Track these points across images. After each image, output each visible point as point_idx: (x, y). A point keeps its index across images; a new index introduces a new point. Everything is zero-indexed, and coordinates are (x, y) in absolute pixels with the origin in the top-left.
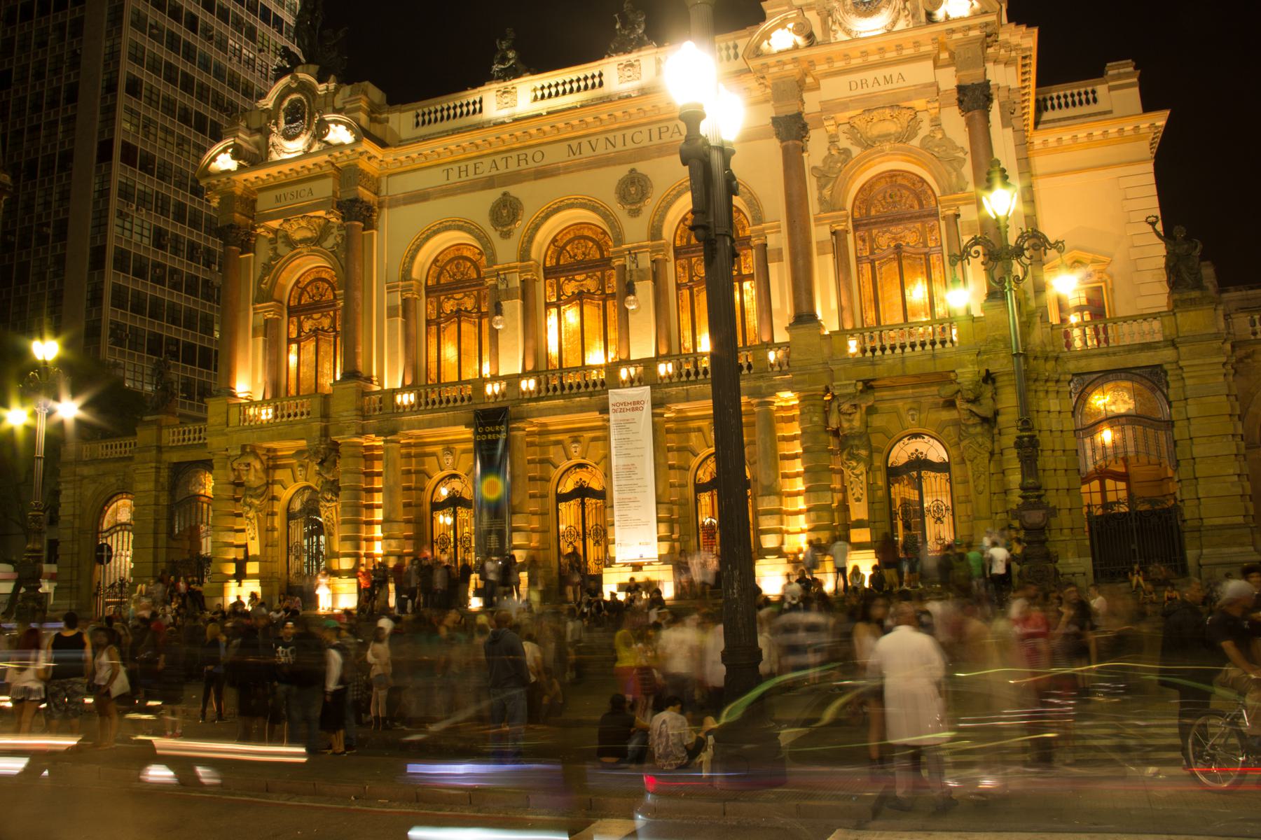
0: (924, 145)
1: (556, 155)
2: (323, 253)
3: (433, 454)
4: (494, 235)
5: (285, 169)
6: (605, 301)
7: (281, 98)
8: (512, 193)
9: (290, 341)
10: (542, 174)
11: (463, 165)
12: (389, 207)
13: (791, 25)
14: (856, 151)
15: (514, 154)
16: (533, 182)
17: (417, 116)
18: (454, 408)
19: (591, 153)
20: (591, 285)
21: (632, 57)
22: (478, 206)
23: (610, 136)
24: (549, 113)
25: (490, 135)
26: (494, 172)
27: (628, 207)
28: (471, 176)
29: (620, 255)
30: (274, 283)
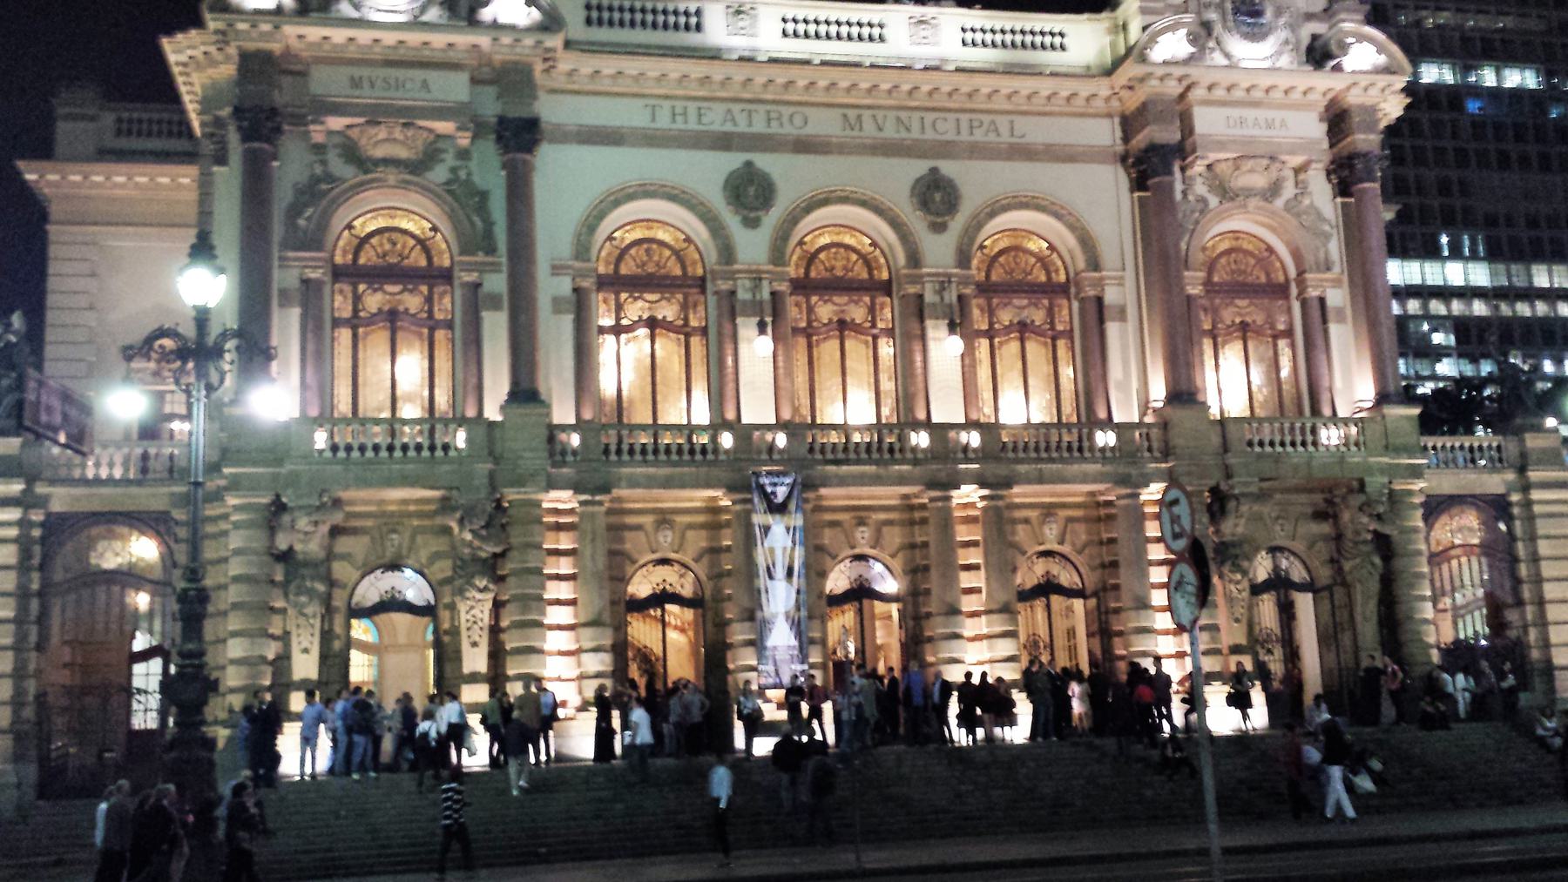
0: (1288, 207)
1: (824, 124)
3: (639, 527)
4: (732, 221)
5: (364, 36)
6: (875, 338)
9: (337, 323)
10: (804, 146)
11: (679, 105)
12: (553, 140)
14: (1213, 201)
15: (762, 108)
18: (705, 463)
20: (858, 314)
21: (929, 11)
22: (708, 172)
23: (903, 115)
24: (824, 63)
25: (717, 71)
26: (729, 127)
27: (931, 218)
28: (693, 125)
30: (323, 225)
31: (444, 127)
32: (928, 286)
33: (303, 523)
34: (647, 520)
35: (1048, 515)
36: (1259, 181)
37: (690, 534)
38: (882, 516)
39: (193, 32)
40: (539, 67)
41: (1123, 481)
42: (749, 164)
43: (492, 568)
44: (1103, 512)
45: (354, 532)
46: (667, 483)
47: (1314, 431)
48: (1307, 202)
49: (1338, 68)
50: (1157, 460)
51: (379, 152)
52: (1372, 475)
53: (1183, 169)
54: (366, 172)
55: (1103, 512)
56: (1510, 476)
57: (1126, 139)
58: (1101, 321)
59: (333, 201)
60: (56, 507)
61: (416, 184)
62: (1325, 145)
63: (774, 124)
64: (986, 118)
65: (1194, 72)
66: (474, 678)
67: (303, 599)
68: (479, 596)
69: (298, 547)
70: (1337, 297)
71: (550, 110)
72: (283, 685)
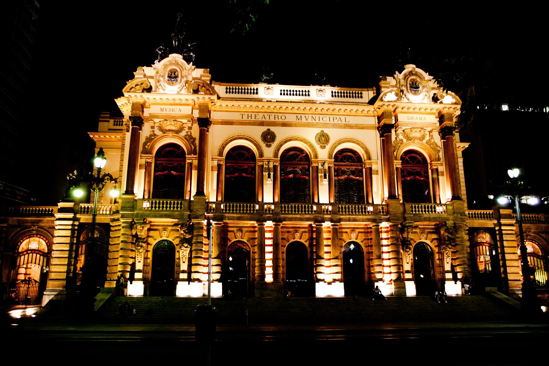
0: (427, 143)
2: (180, 138)
4: (263, 145)
7: (166, 66)
8: (271, 130)
10: (284, 125)
12: (214, 124)
13: (393, 93)
14: (405, 141)
15: (273, 114)
16: (281, 127)
17: (227, 89)
19: (306, 121)
21: (323, 87)
22: (257, 132)
23: (314, 116)
26: (263, 120)
28: (253, 119)
29: (317, 162)
31: (185, 121)
32: (320, 164)
33: (139, 227)
34: (235, 229)
35: (353, 231)
36: (418, 135)
37: (247, 233)
38: (303, 230)
39: (122, 98)
40: (210, 105)
41: (374, 221)
42: (269, 129)
43: (189, 242)
44: (369, 230)
45: (155, 230)
46: (239, 219)
47: (435, 208)
48: (433, 141)
49: (441, 103)
50: (384, 215)
51: (168, 128)
52: (448, 221)
53: (396, 131)
54: (164, 133)
55: (369, 230)
56: (496, 222)
57: (379, 123)
58: (371, 174)
59: (154, 142)
60: (82, 221)
61: (177, 136)
62: (438, 124)
63: (277, 119)
64: (338, 117)
65: (397, 104)
66: (183, 272)
67: (140, 247)
68: (185, 249)
69: (138, 234)
70: (442, 168)
71: (215, 116)
72: (133, 271)
